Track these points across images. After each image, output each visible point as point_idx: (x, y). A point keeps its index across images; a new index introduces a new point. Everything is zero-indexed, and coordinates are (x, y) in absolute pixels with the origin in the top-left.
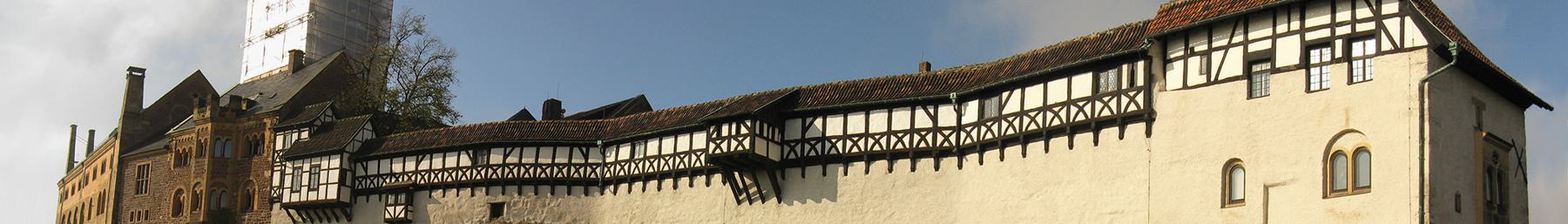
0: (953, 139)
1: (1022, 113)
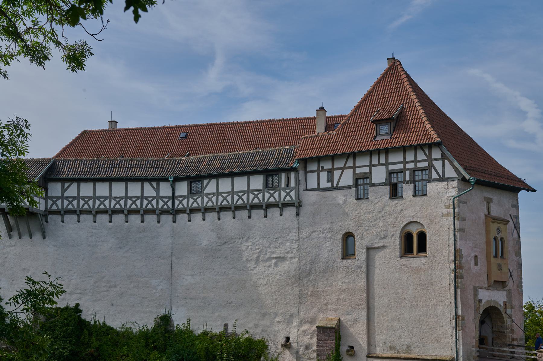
0: (170, 204)
1: (217, 194)
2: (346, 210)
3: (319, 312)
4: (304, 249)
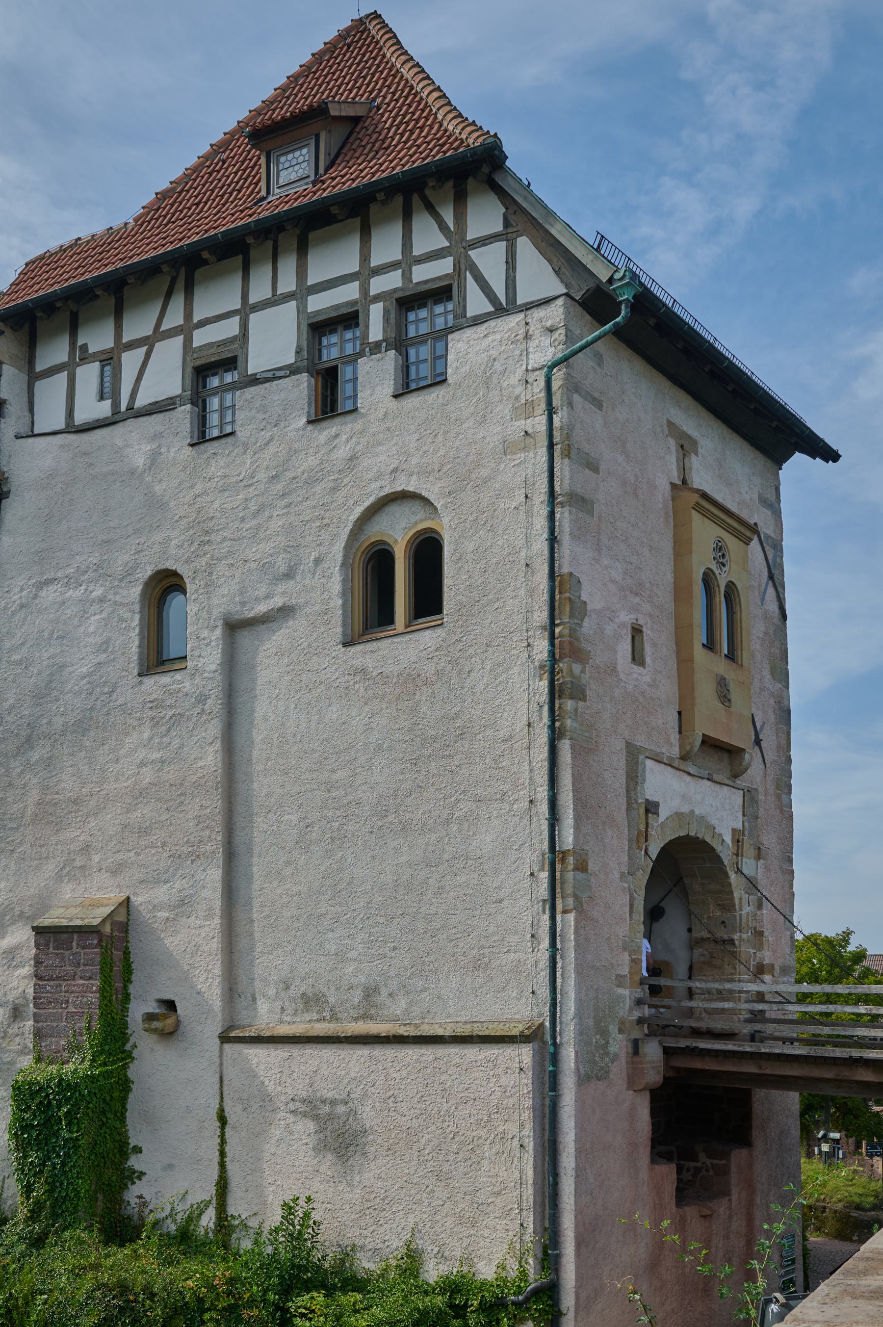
2: (158, 489)
3: (59, 877)
4: (15, 649)
